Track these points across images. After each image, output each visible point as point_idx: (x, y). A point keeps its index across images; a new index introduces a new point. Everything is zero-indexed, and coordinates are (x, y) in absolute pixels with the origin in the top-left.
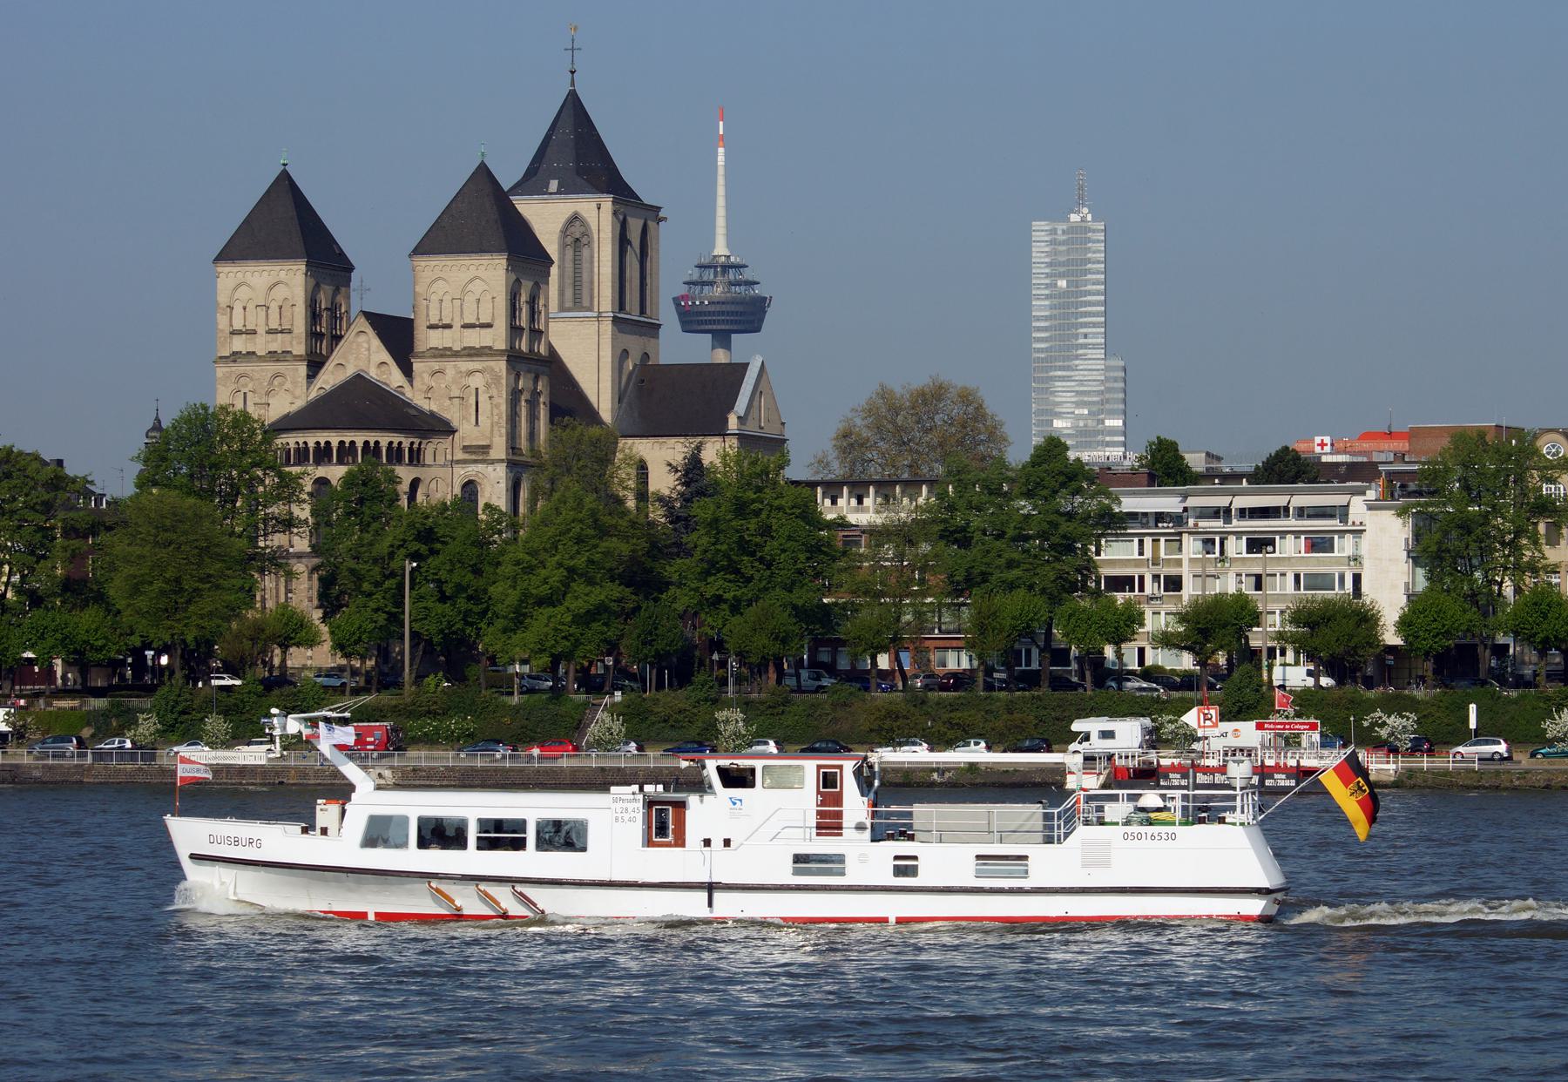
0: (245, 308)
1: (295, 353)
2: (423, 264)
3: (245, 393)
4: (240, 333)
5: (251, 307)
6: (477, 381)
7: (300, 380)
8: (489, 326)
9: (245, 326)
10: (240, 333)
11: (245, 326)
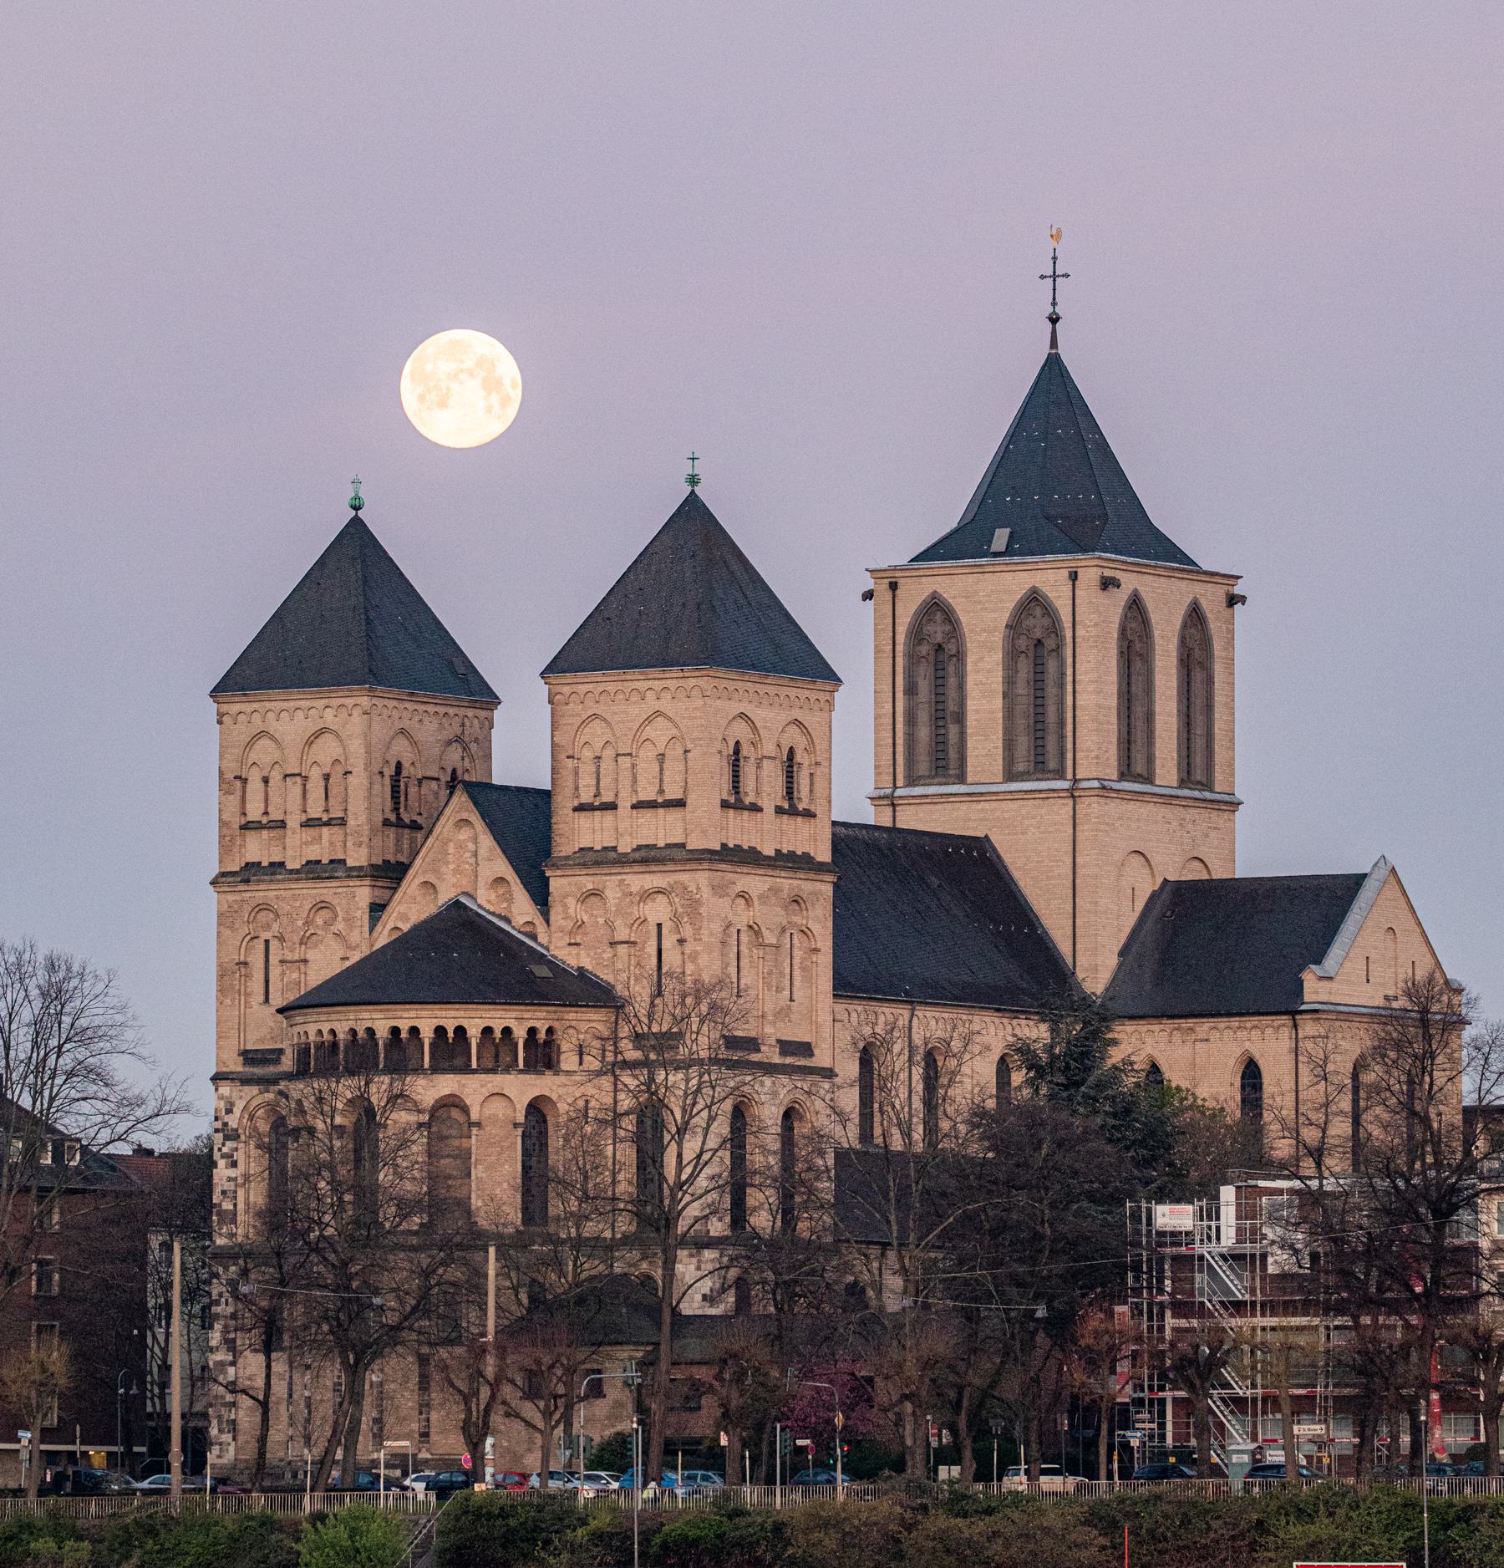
0: (266, 781)
1: (350, 863)
2: (566, 690)
3: (267, 942)
4: (256, 826)
5: (275, 777)
6: (657, 911)
7: (358, 914)
8: (680, 804)
9: (266, 813)
10: (256, 826)
11: (266, 813)
